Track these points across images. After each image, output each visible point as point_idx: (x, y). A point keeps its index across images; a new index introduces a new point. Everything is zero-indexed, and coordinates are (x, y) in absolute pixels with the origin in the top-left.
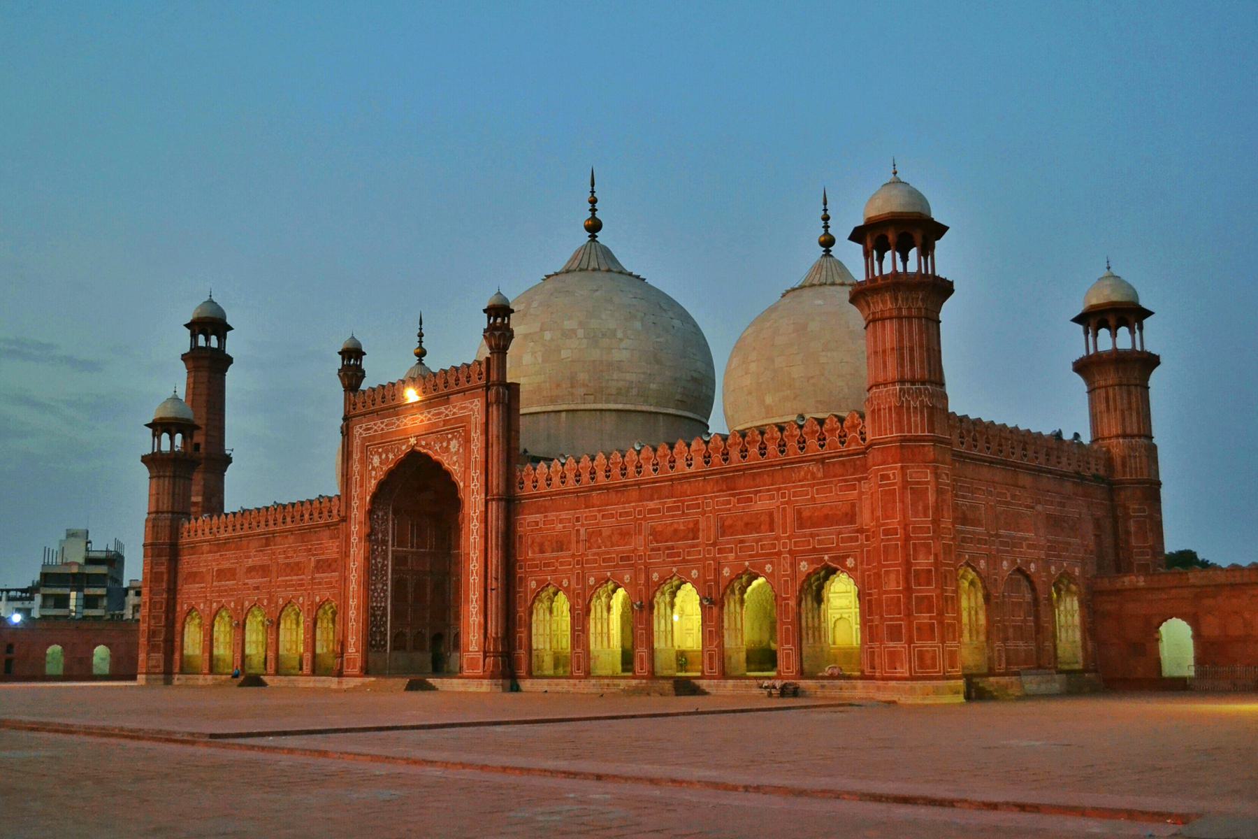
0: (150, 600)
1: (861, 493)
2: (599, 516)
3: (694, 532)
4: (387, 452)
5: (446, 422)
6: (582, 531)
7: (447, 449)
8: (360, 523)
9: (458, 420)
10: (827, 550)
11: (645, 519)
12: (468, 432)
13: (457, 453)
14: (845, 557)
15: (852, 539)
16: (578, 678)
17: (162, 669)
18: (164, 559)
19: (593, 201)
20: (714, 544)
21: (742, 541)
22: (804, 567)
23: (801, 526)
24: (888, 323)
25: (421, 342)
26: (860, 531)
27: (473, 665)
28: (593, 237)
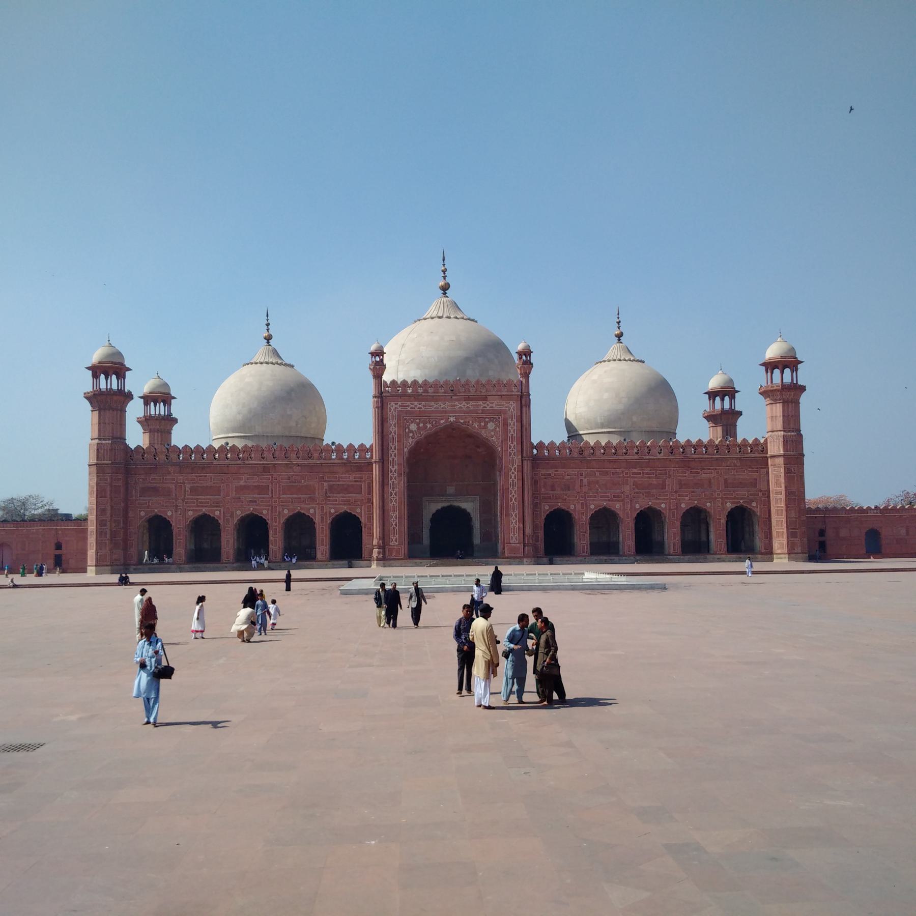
0: (112, 507)
3: (663, 486)
5: (483, 411)
6: (585, 481)
7: (485, 427)
9: (494, 411)
10: (741, 498)
12: (506, 419)
15: (754, 494)
16: (585, 557)
17: (122, 561)
18: (120, 476)
19: (444, 271)
20: (676, 492)
22: (729, 506)
24: (791, 405)
26: (761, 491)
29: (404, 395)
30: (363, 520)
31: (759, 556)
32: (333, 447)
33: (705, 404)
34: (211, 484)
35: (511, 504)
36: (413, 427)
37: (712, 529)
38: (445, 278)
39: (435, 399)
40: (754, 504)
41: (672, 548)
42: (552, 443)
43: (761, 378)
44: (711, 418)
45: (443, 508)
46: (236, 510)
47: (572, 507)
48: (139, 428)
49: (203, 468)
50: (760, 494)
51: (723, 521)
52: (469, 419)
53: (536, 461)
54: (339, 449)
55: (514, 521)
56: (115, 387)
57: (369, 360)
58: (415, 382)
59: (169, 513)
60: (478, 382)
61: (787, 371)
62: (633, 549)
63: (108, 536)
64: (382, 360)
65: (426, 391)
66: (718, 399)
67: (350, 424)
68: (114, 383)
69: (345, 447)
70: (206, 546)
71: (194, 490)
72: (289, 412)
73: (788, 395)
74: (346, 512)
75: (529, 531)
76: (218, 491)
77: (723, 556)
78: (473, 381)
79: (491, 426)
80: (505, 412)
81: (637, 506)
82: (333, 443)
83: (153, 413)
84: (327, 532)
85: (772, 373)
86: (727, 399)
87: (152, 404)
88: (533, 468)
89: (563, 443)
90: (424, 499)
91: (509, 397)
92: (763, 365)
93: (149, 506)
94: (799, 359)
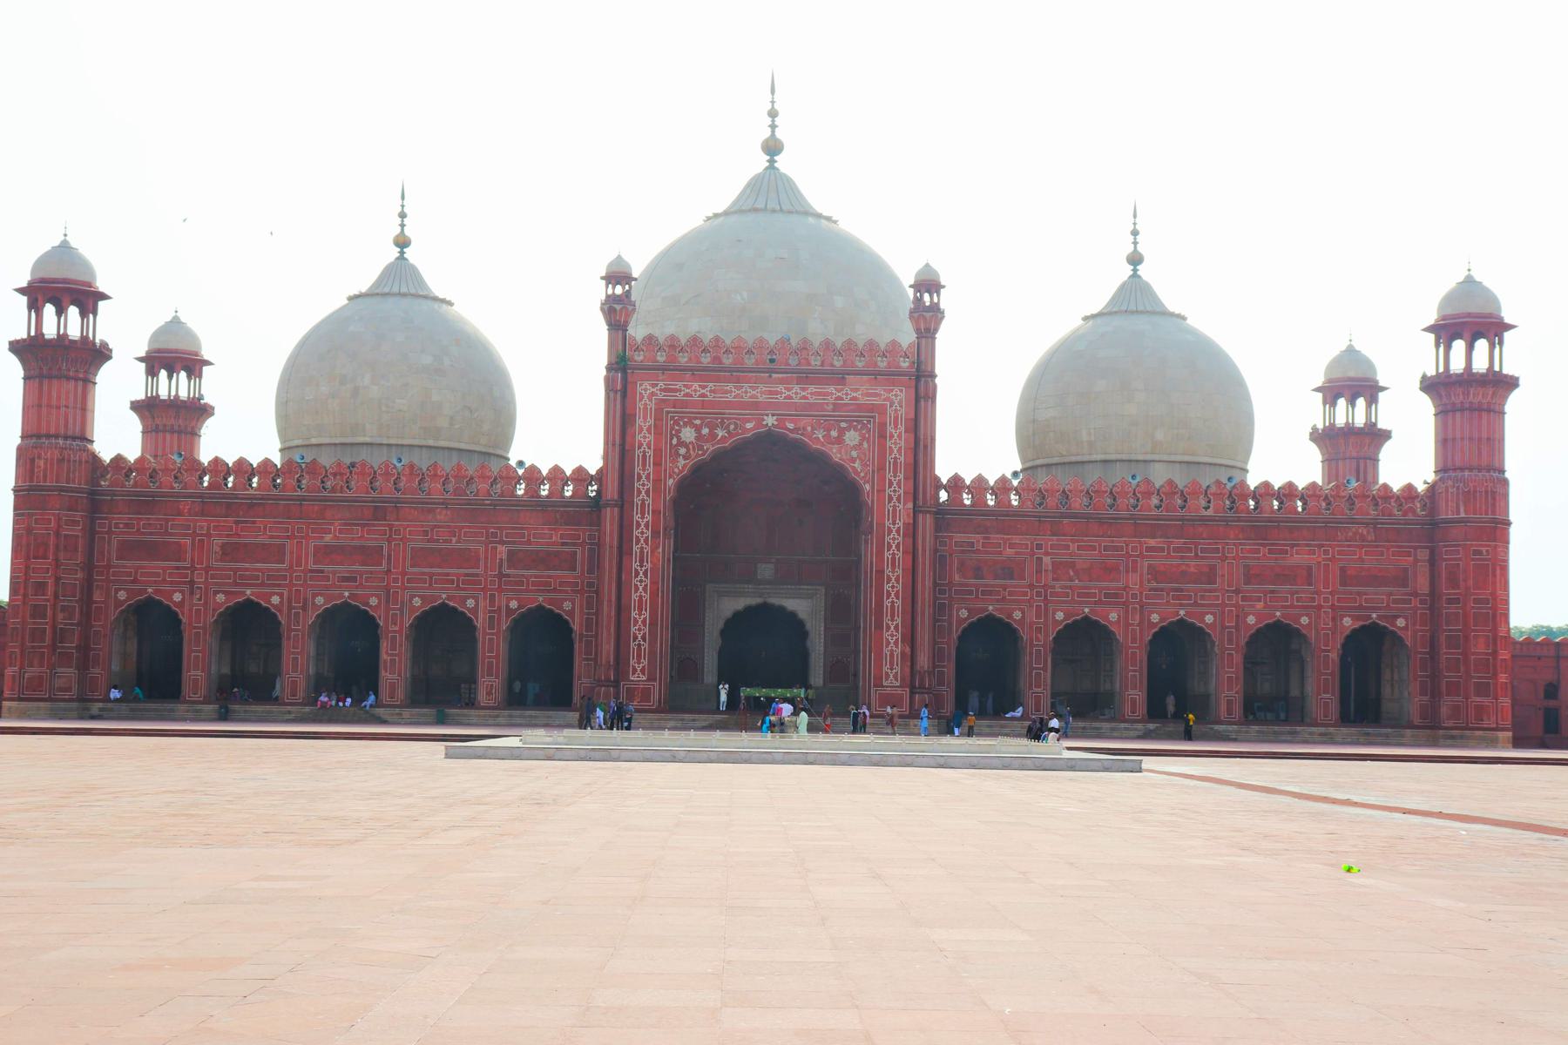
0: (57, 579)
1: (1416, 561)
2: (1073, 547)
3: (1210, 576)
4: (712, 427)
5: (836, 407)
6: (1047, 560)
7: (840, 440)
8: (656, 512)
9: (860, 407)
10: (1374, 609)
11: (1142, 556)
12: (883, 426)
13: (858, 447)
14: (1397, 617)
15: (1405, 602)
17: (74, 692)
19: (773, 114)
20: (1237, 591)
21: (1272, 592)
22: (1347, 622)
23: (1343, 584)
25: (403, 226)
26: (1415, 594)
27: (886, 700)
28: (772, 162)
29: (670, 369)
30: (575, 627)
31: (1409, 732)
32: (521, 472)
33: (1314, 414)
34: (268, 541)
35: (887, 603)
36: (688, 434)
37: (1309, 672)
38: (773, 127)
39: (737, 374)
40: (1401, 622)
41: (1223, 707)
42: (980, 481)
43: (1425, 358)
44: (1328, 439)
45: (749, 610)
46: (315, 595)
47: (1017, 615)
48: (135, 425)
49: (252, 506)
50: (1415, 602)
51: (1334, 656)
52: (804, 421)
53: (947, 518)
54: (533, 476)
55: (892, 639)
56: (74, 329)
57: (600, 291)
58: (695, 341)
59: (177, 597)
60: (827, 345)
61: (1482, 345)
62: (1142, 709)
63: (48, 641)
64: (627, 294)
65: (717, 359)
66: (1342, 402)
67: (559, 428)
68: (73, 324)
69: (545, 472)
70: (253, 668)
71: (230, 552)
72: (435, 398)
73: (1477, 396)
74: (540, 608)
75: (923, 661)
76: (277, 553)
77: (1331, 729)
78: (817, 343)
79: (852, 437)
80: (882, 410)
81: (1155, 618)
82: (521, 463)
83: (163, 393)
84: (503, 647)
85: (1448, 348)
86: (1361, 403)
87: (163, 374)
88: (938, 528)
89: (1003, 480)
90: (709, 587)
91: (890, 376)
92: (1429, 329)
93: (135, 581)
94: (1507, 320)
